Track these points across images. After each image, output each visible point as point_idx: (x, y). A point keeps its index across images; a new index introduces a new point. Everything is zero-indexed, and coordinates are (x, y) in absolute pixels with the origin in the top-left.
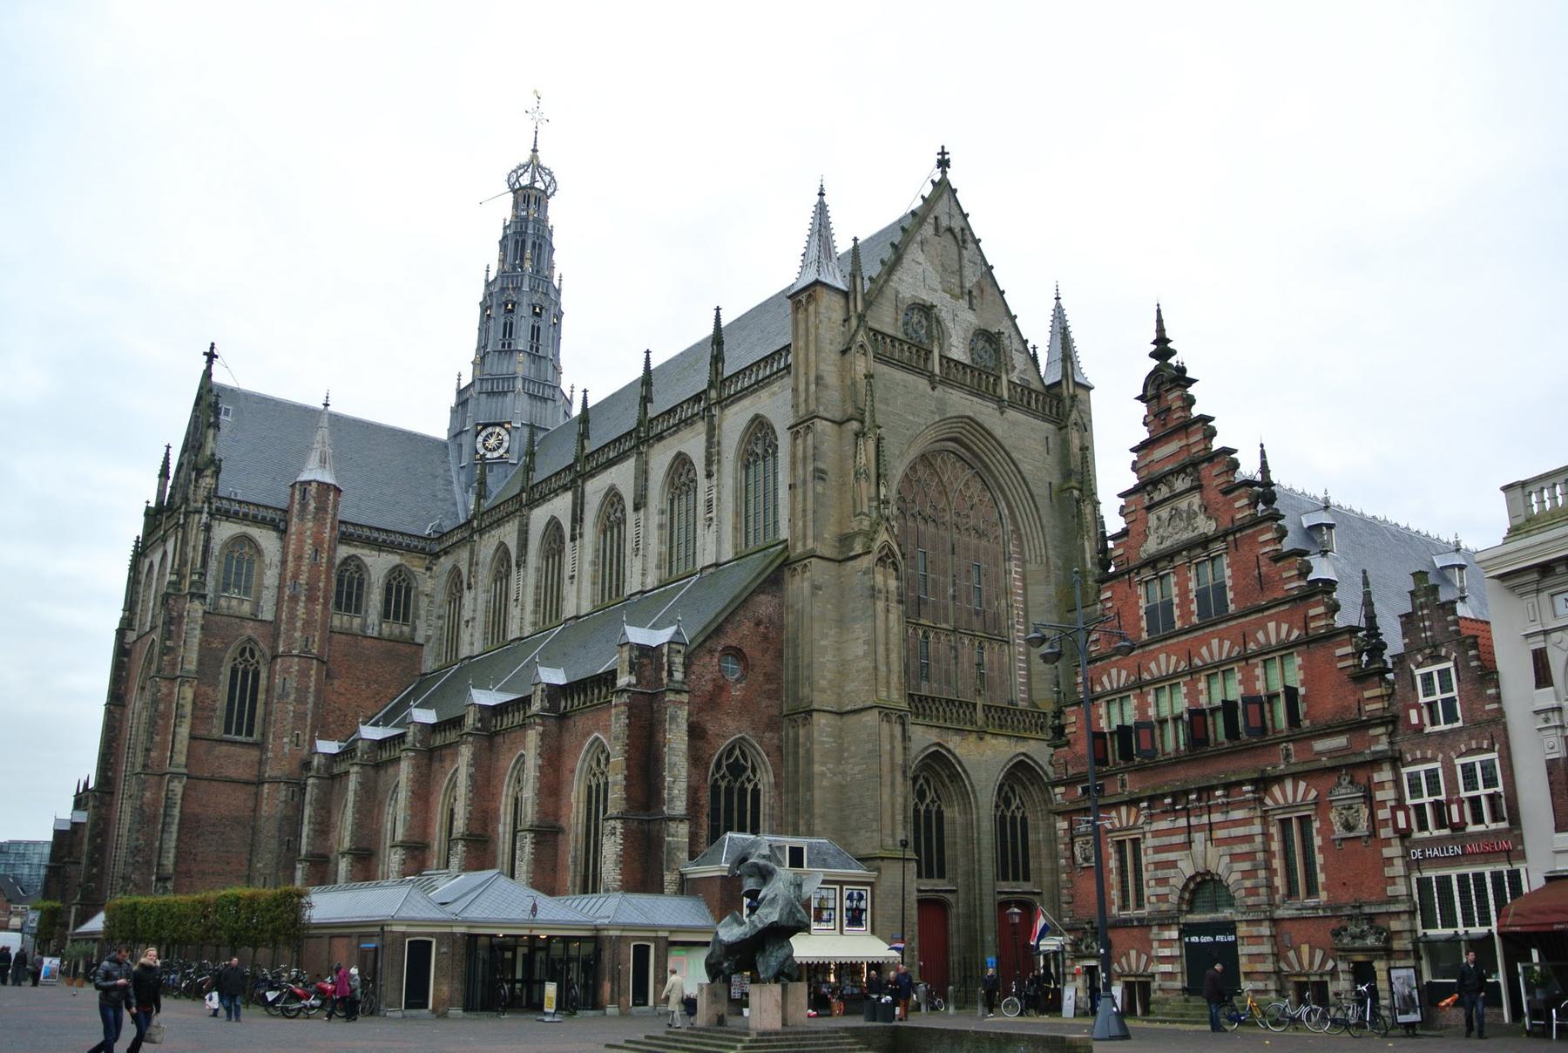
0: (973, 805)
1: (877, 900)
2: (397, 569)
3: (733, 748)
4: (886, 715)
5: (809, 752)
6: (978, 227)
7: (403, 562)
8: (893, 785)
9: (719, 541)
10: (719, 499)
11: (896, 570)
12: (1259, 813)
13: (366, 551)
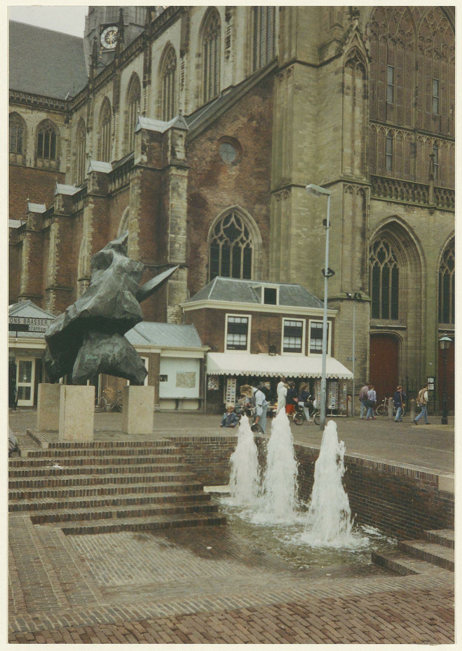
0: (423, 265)
1: (336, 331)
2: (43, 122)
3: (230, 216)
4: (350, 188)
5: (288, 218)
7: (49, 117)
8: (353, 243)
9: (234, 69)
10: (235, 36)
11: (364, 70)
13: (24, 110)
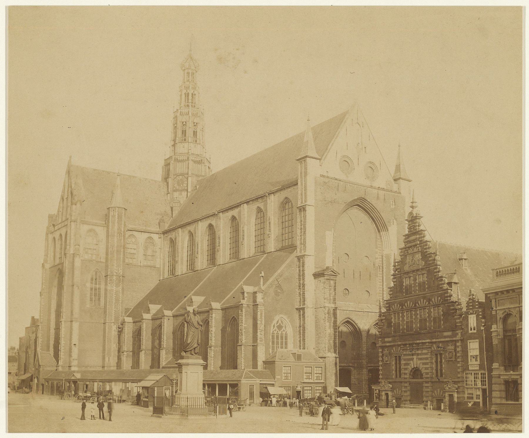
12: (430, 351)
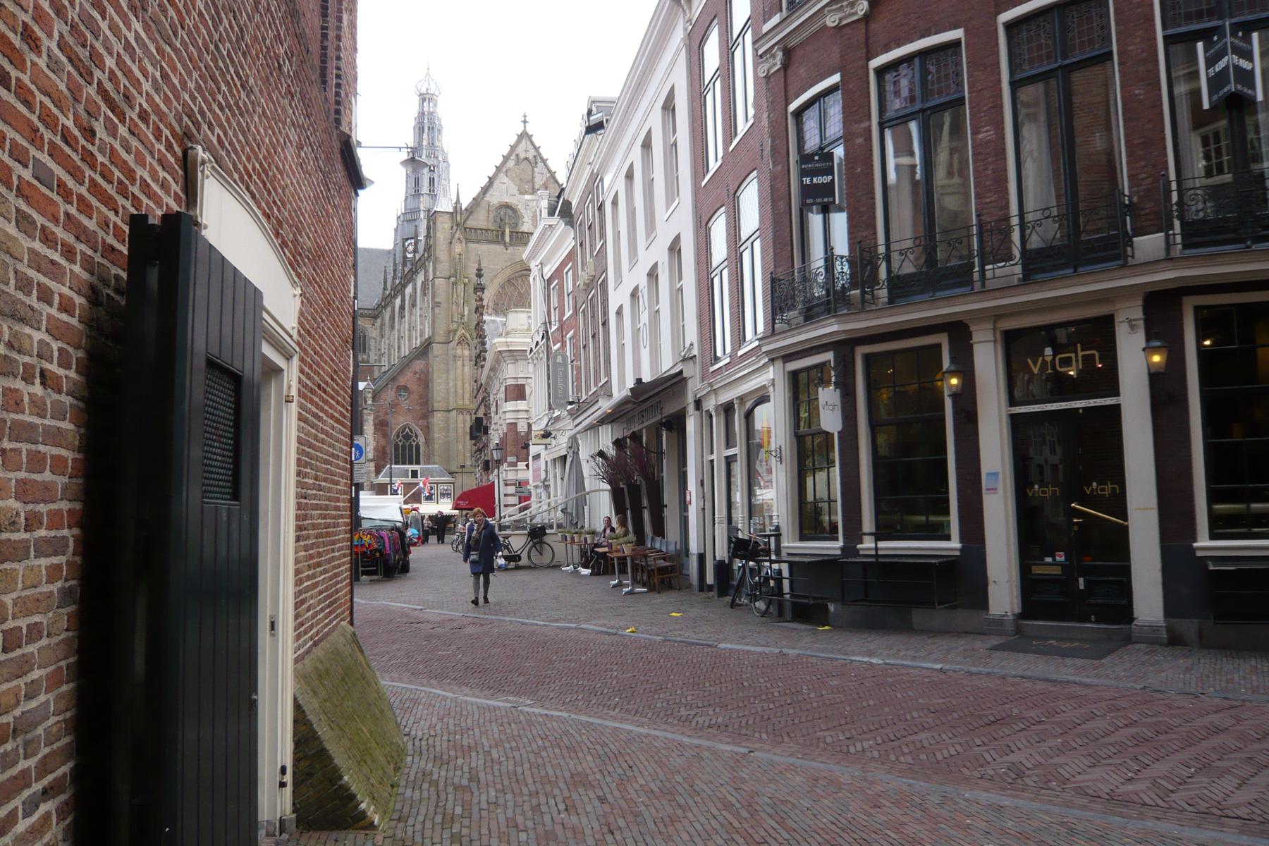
6: (545, 153)
